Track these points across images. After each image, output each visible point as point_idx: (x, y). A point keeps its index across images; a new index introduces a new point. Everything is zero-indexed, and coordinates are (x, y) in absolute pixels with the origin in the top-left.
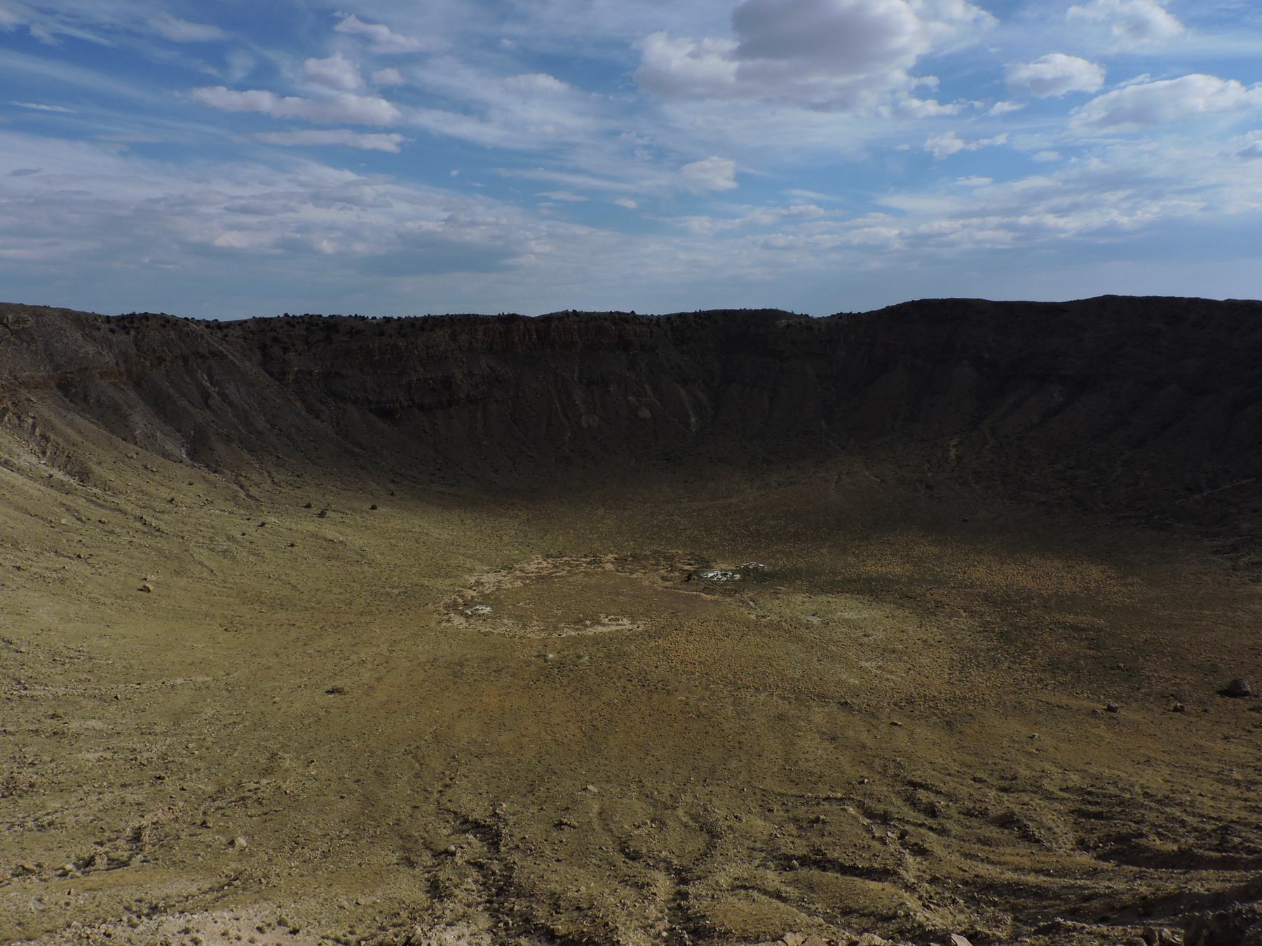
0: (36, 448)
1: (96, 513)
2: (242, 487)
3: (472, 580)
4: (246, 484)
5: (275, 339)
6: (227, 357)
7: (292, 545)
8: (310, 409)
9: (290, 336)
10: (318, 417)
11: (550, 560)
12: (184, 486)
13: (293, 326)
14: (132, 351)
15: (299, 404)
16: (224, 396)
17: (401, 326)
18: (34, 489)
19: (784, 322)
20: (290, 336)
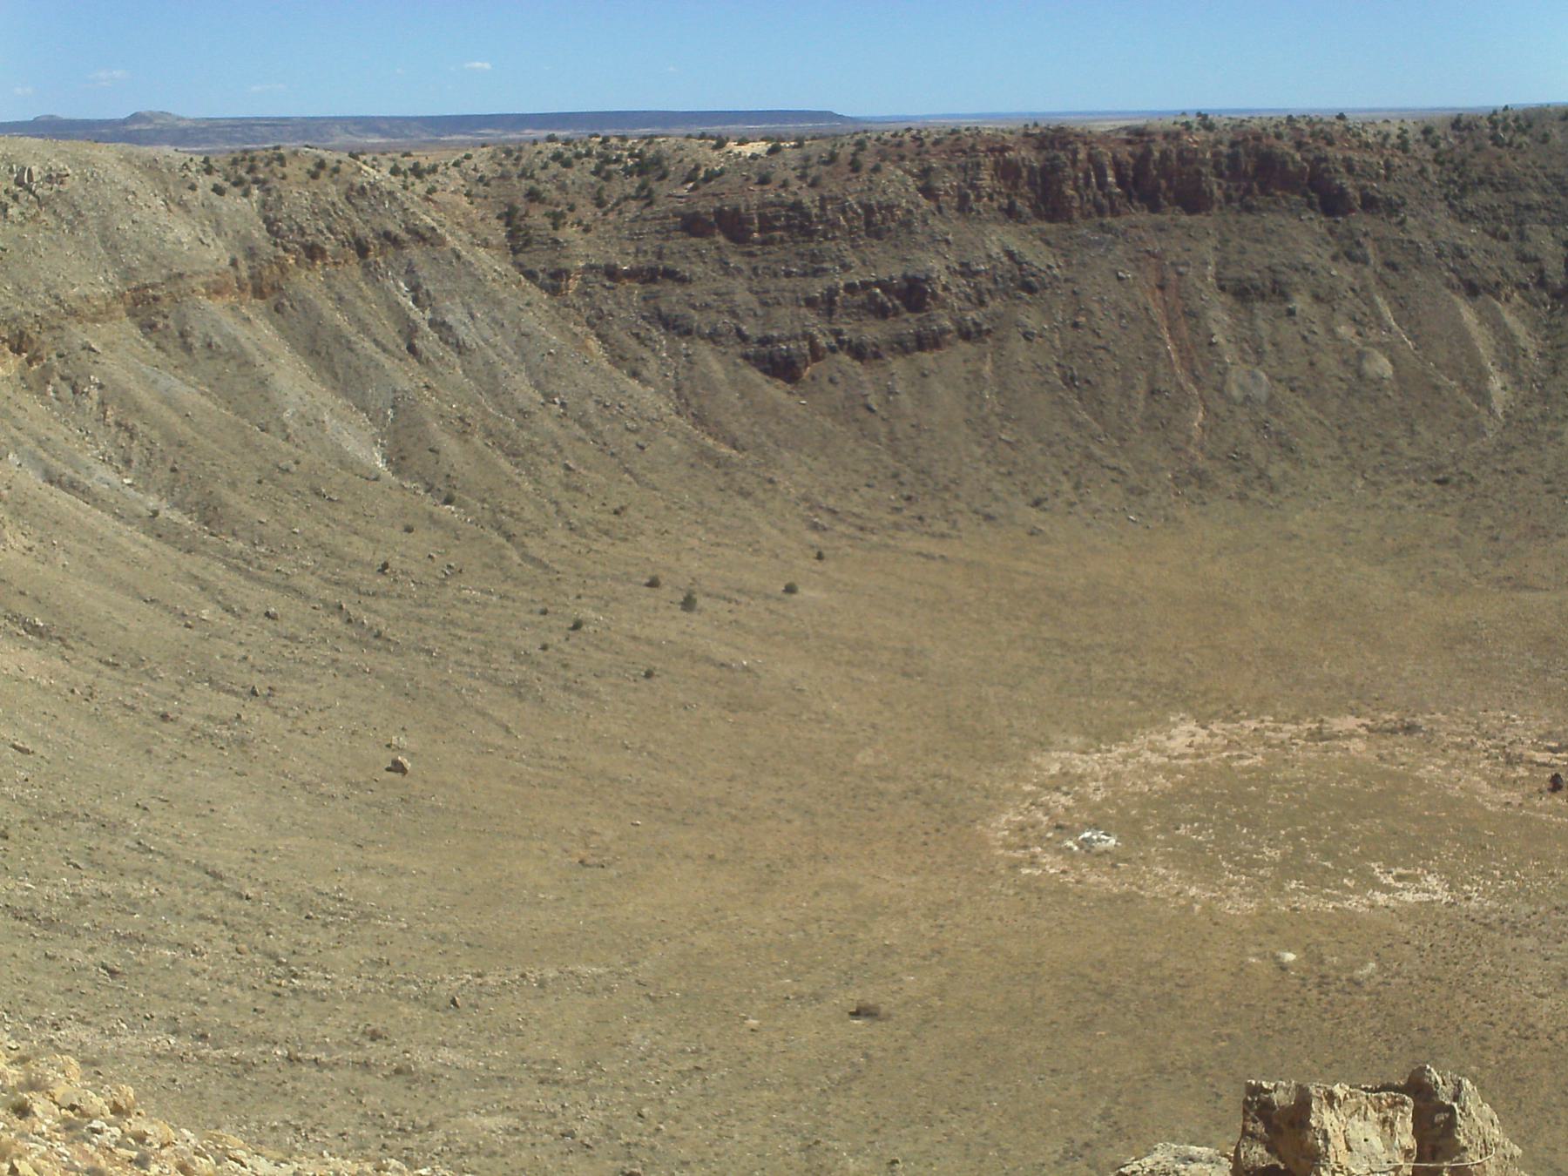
0: (111, 451)
1: (256, 597)
2: (509, 537)
3: (1055, 769)
4: (516, 528)
5: (533, 196)
6: (443, 242)
7: (649, 675)
8: (618, 359)
9: (562, 188)
10: (634, 374)
11: (1216, 727)
12: (397, 534)
13: (567, 164)
14: (259, 234)
15: (594, 344)
17: (807, 159)
18: (135, 541)
20: (562, 188)
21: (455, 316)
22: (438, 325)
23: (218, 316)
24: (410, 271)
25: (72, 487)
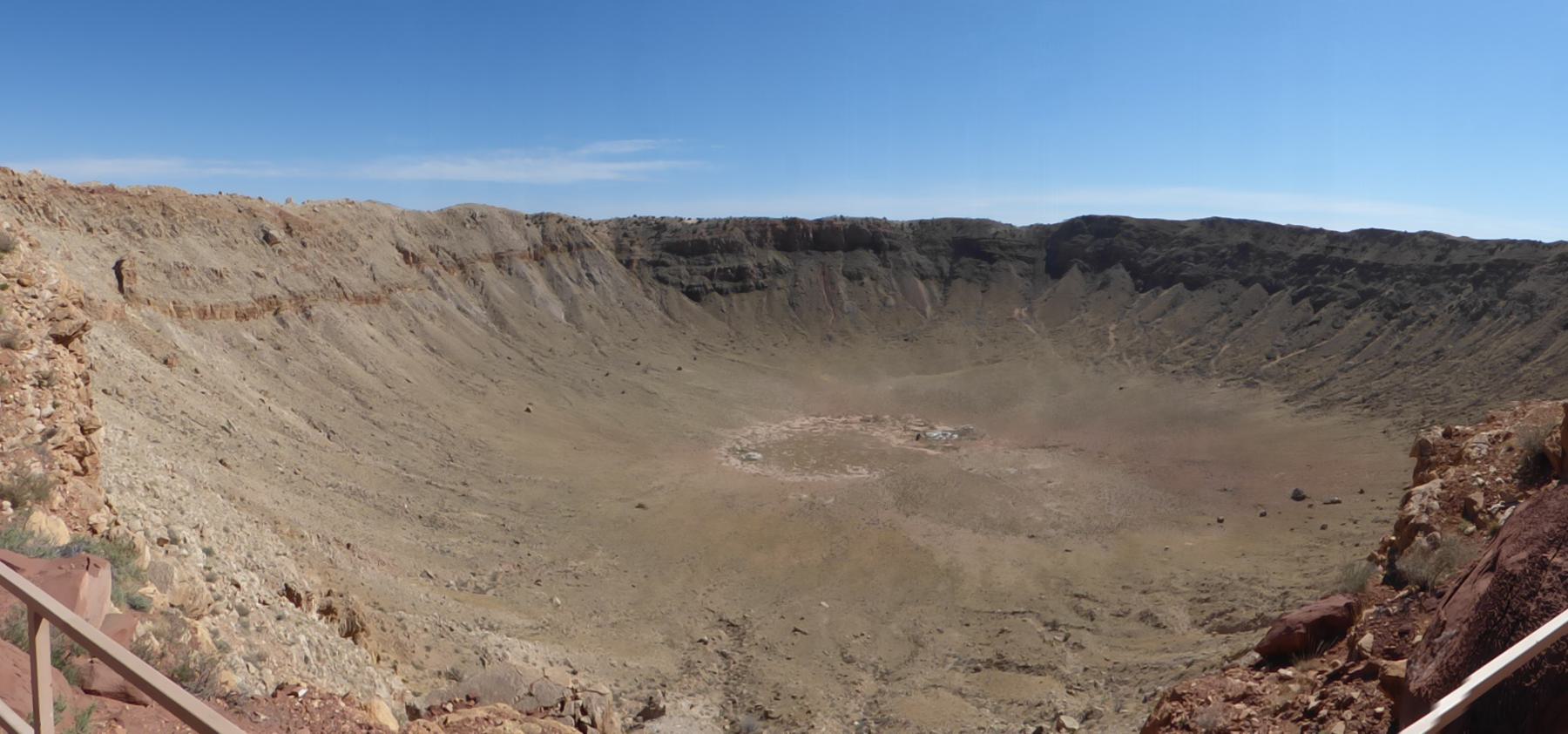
16: (589, 275)
19: (993, 230)
21: (595, 272)
22: (589, 275)
23: (523, 266)
24: (582, 257)
25: (464, 311)
